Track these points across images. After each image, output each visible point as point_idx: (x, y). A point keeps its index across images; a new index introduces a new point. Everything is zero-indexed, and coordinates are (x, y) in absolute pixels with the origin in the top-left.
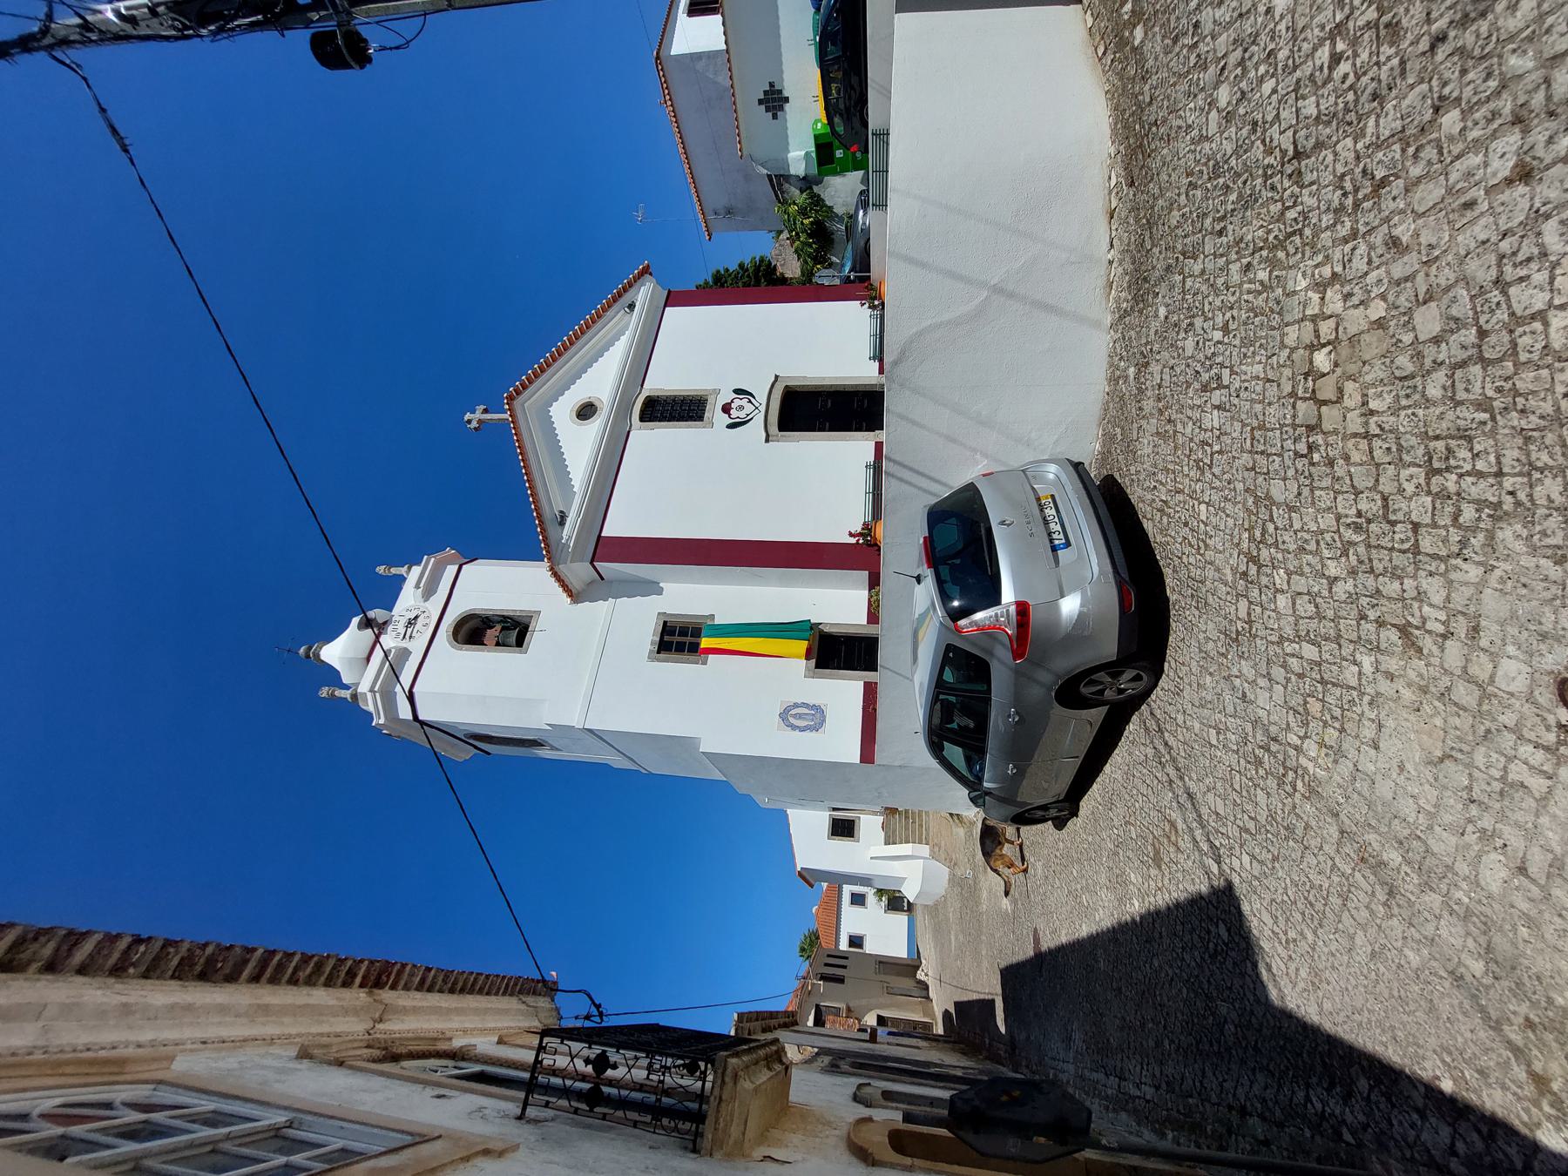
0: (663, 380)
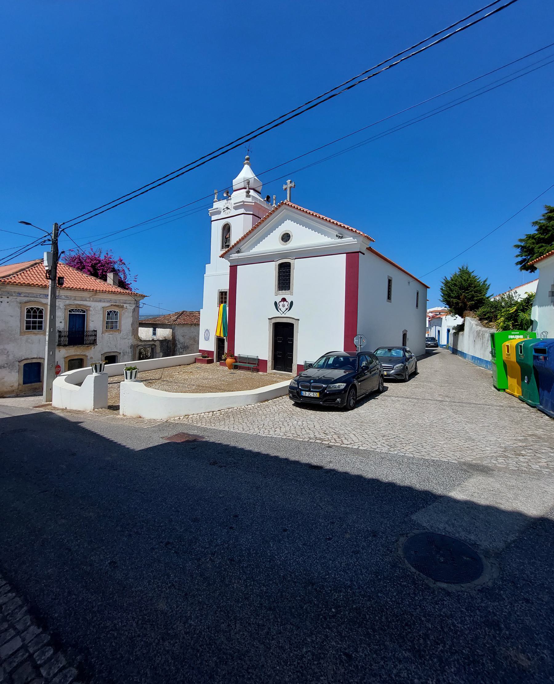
0: (299, 268)
